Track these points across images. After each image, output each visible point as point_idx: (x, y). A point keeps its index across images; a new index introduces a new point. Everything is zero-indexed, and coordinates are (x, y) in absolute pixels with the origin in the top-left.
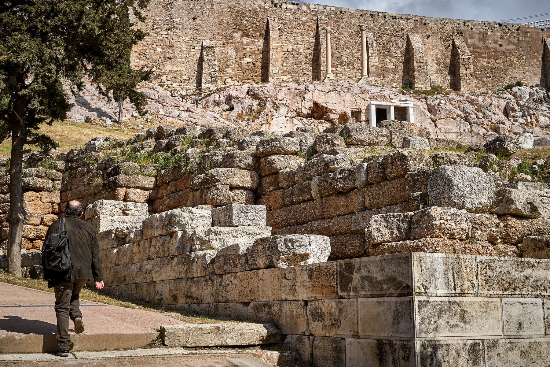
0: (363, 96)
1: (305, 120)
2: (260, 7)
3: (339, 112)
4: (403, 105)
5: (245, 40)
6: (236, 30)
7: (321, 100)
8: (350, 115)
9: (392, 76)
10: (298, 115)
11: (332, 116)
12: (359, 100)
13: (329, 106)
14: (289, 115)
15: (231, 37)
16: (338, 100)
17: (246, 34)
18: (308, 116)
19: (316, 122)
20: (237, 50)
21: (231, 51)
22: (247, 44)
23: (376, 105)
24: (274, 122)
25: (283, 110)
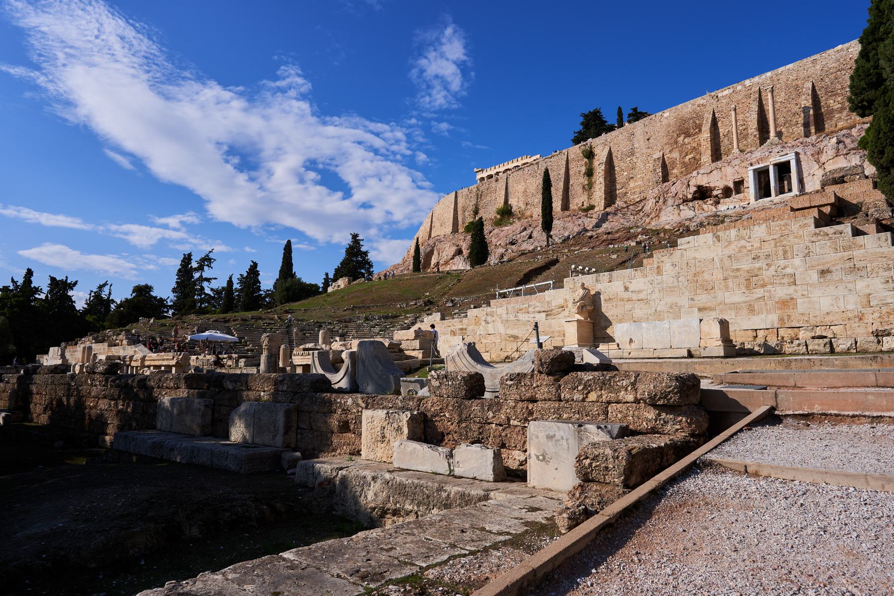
0: (743, 164)
1: (690, 204)
2: (699, 106)
3: (722, 186)
4: (784, 159)
5: (686, 140)
6: (679, 136)
7: (703, 181)
8: (731, 185)
9: (837, 116)
10: (684, 202)
11: (715, 193)
12: (740, 170)
13: (712, 185)
14: (676, 203)
15: (676, 142)
16: (720, 176)
17: (688, 135)
18: (694, 199)
19: (700, 202)
20: (681, 152)
21: (676, 155)
22: (689, 143)
23: (754, 170)
24: (663, 213)
25: (670, 202)
